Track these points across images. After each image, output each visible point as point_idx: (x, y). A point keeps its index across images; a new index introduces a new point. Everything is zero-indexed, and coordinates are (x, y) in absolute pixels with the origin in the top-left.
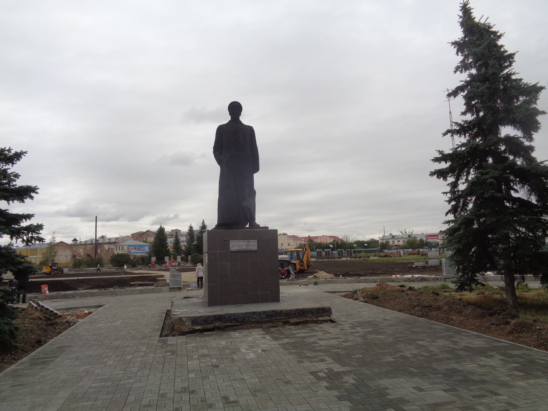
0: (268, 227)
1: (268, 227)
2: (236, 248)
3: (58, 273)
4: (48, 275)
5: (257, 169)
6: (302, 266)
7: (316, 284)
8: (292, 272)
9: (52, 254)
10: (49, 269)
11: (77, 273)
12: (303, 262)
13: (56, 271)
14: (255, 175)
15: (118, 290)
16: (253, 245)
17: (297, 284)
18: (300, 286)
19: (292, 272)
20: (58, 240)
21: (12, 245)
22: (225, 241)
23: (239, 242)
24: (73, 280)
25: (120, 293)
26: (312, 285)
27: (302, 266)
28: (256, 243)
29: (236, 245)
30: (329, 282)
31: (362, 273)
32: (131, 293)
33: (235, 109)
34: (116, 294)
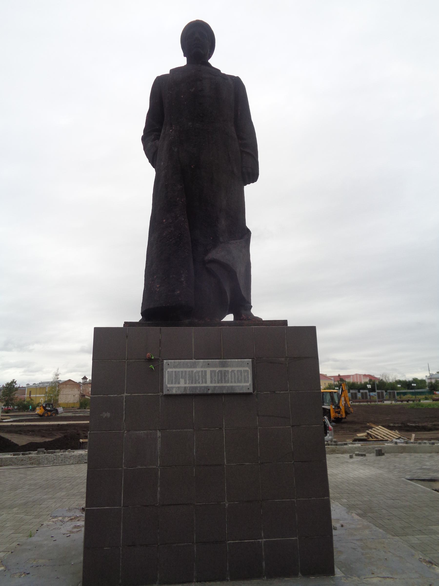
0: (285, 322)
1: (285, 322)
2: (182, 384)
3: (51, 415)
4: (41, 417)
5: (252, 175)
6: (339, 413)
7: (380, 453)
8: (330, 426)
9: (55, 393)
10: (43, 410)
11: (74, 415)
12: (339, 407)
13: (49, 413)
14: (248, 189)
15: (43, 456)
16: (238, 376)
17: (343, 453)
18: (351, 457)
19: (330, 426)
20: (63, 378)
21: (15, 383)
22: (150, 360)
23: (194, 366)
24: (53, 425)
25: (46, 462)
26: (371, 457)
27: (339, 413)
28: (249, 369)
29: (181, 376)
30: (403, 450)
31: (429, 425)
32: (64, 462)
33: (198, 40)
34: (39, 463)
